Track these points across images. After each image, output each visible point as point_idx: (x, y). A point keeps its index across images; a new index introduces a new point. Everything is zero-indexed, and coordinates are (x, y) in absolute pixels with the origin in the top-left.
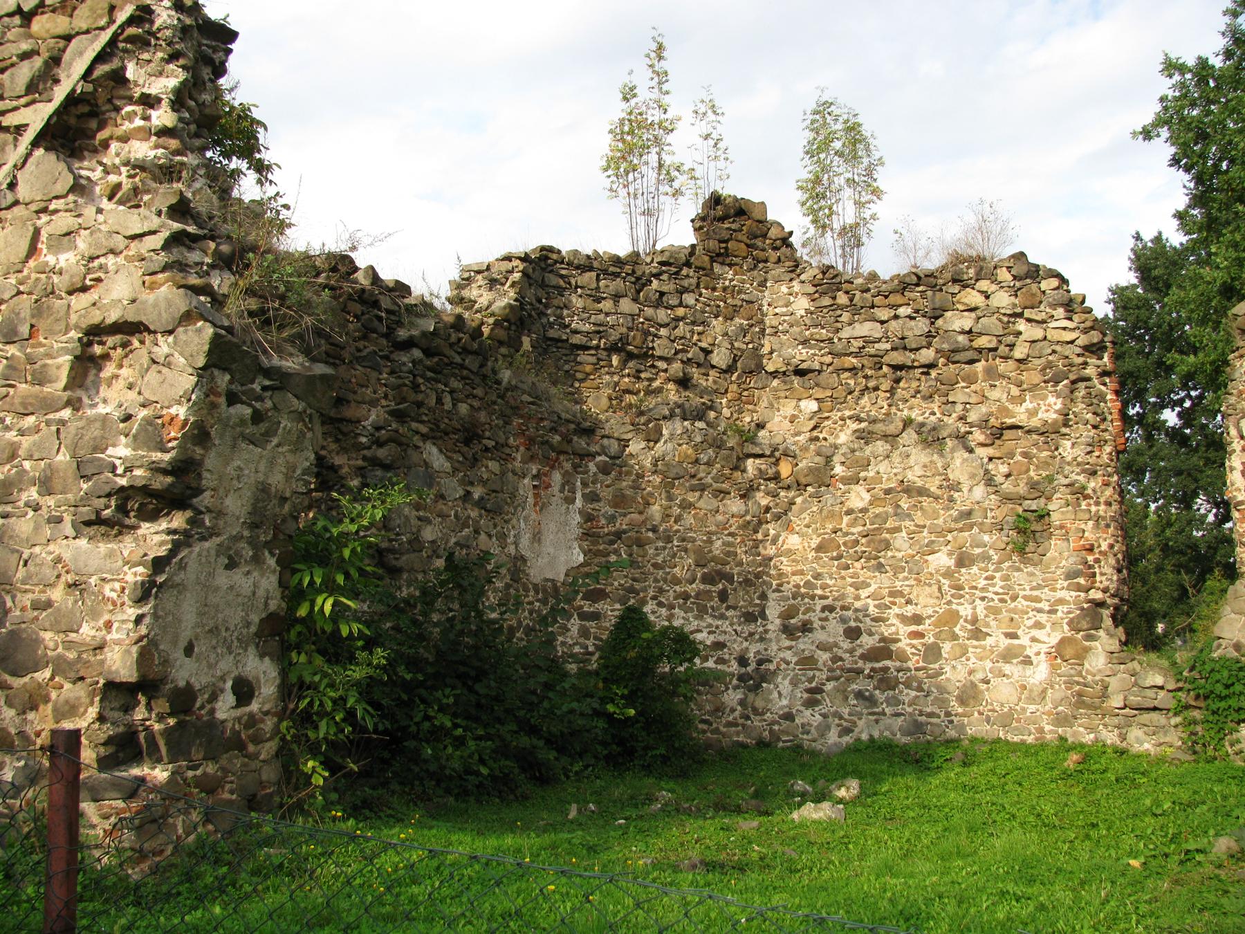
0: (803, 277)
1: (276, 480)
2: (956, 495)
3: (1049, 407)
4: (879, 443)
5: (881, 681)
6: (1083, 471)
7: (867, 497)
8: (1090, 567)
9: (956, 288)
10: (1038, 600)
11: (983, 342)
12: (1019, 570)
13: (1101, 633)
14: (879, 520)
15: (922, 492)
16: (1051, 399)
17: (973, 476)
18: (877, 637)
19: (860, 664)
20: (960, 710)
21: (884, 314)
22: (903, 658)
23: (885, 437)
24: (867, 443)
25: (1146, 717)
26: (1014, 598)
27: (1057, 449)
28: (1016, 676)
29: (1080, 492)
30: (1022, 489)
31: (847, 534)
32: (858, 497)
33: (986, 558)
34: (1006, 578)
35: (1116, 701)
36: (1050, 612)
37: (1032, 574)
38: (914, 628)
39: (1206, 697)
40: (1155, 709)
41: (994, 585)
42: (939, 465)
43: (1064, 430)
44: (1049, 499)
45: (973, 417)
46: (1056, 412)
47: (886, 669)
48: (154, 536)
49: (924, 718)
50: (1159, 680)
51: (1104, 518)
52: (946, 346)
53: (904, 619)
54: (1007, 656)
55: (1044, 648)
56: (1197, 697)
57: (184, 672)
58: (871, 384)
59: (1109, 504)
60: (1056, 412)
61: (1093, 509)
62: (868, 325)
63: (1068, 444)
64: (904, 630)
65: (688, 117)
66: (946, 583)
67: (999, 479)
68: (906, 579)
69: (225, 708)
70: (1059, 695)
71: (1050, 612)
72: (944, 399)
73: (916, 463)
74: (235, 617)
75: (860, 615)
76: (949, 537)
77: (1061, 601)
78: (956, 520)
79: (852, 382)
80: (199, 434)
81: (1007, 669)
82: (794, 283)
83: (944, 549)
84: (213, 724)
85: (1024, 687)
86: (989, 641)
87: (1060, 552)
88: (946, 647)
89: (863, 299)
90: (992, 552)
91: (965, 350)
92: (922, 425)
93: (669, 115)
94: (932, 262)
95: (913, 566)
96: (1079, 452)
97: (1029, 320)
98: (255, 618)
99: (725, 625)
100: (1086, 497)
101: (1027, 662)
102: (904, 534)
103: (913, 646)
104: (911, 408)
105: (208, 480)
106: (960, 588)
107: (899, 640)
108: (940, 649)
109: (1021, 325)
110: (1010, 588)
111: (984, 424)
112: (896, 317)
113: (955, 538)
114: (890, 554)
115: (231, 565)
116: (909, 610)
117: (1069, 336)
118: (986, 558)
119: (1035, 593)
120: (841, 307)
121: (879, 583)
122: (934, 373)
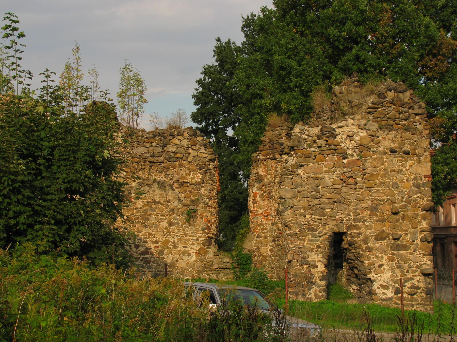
0: (122, 131)
2: (169, 204)
3: (198, 177)
4: (146, 187)
5: (145, 261)
6: (208, 198)
7: (142, 204)
8: (209, 227)
9: (171, 138)
10: (193, 236)
11: (179, 155)
12: (188, 227)
13: (212, 246)
14: (145, 211)
15: (159, 203)
16: (199, 175)
17: (174, 198)
18: (144, 248)
19: (139, 256)
20: (169, 270)
21: (148, 145)
22: (152, 254)
23: (148, 185)
24: (142, 187)
25: (224, 271)
26: (186, 236)
27: (200, 190)
28: (186, 259)
29: (207, 205)
30: (189, 202)
31: (135, 216)
32: (139, 204)
33: (178, 223)
34: (184, 230)
35: (216, 266)
36: (196, 240)
37: (192, 229)
38: (155, 245)
39: (240, 265)
40: (226, 268)
41: (180, 232)
42: (164, 194)
43: (202, 185)
44: (197, 206)
45: (174, 179)
46: (200, 179)
47: (147, 258)
49: (158, 273)
50: (228, 260)
51: (213, 212)
52: (167, 156)
53: (153, 242)
54: (184, 253)
55: (195, 251)
56: (238, 265)
58: (143, 167)
59: (215, 208)
60: (200, 179)
61: (210, 210)
62: (143, 148)
63: (204, 189)
64: (153, 246)
65: (86, 75)
66: (166, 231)
67: (182, 199)
68: (154, 230)
70: (199, 265)
71: (196, 240)
72: (166, 173)
73: (156, 194)
75: (139, 241)
76: (167, 217)
77: (200, 237)
78: (169, 212)
79: (137, 166)
81: (184, 257)
82: (119, 133)
83: (166, 221)
85: (188, 263)
86: (178, 249)
87: (200, 222)
88: (166, 251)
89: (141, 140)
90: (180, 222)
91: (173, 158)
92: (159, 182)
93: (80, 73)
94: (163, 126)
95: (156, 226)
96: (207, 192)
97: (193, 149)
100: (209, 206)
101: (190, 255)
102: (153, 216)
103: (155, 250)
104: (155, 175)
106: (170, 233)
107: (151, 249)
108: (163, 251)
109: (190, 151)
110: (185, 233)
111: (178, 181)
112: (152, 146)
113: (169, 217)
114: (148, 222)
116: (154, 239)
117: (205, 156)
118: (178, 223)
119: (192, 234)
120: (134, 142)
121: (145, 231)
122: (163, 165)
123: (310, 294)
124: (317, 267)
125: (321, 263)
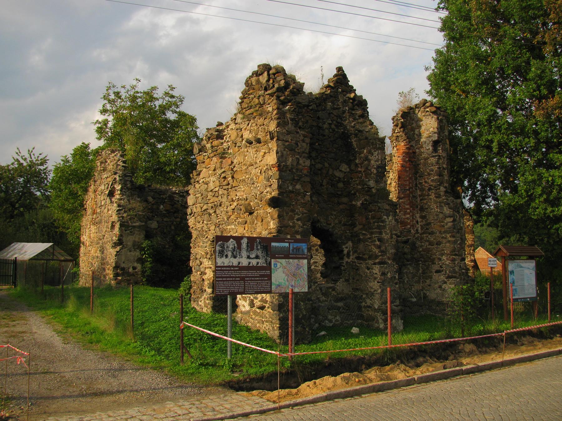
1: (137, 240)
48: (118, 248)
57: (123, 265)
69: (131, 270)
74: (132, 258)
80: (121, 235)
84: (128, 272)
98: (136, 258)
99: (318, 257)
105: (124, 241)
115: (130, 251)
123: (201, 301)
124: (206, 274)
125: (210, 270)
